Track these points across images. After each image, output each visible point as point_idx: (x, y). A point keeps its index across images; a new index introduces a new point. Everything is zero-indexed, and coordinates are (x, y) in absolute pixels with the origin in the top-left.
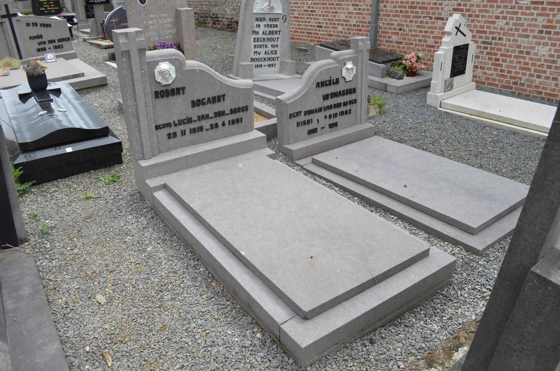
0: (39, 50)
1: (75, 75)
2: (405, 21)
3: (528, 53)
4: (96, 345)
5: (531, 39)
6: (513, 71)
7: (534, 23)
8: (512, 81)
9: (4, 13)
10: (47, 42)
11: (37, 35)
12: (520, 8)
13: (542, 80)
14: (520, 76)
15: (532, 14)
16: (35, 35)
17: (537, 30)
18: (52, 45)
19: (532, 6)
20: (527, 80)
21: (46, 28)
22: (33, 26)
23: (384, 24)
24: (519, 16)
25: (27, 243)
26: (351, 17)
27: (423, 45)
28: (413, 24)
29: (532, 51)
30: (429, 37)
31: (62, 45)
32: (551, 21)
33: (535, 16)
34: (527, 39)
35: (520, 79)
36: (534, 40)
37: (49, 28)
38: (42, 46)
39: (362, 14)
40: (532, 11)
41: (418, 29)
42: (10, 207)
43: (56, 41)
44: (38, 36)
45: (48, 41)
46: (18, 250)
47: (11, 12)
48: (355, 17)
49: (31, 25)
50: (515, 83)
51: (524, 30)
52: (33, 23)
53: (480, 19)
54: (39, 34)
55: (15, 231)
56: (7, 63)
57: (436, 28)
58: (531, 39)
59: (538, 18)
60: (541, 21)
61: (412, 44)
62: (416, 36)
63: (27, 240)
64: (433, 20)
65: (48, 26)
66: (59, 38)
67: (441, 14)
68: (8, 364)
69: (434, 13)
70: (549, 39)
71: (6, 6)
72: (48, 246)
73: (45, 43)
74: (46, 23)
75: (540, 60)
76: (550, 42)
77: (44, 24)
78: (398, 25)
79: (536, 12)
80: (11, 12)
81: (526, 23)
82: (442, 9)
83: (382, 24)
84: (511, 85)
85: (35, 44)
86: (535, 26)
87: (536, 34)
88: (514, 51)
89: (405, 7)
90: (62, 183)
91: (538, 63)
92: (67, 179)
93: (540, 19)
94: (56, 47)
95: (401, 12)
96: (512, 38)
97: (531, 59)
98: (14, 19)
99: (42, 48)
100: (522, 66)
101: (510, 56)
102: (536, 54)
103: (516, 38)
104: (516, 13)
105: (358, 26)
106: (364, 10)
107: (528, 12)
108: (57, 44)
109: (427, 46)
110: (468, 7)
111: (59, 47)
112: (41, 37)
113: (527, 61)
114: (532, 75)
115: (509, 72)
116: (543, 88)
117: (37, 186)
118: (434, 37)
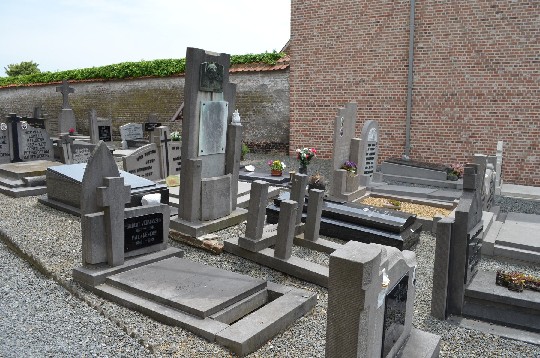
2: (432, 144)
3: (523, 160)
5: (524, 152)
6: (515, 171)
7: (525, 143)
8: (514, 177)
12: (515, 135)
13: (534, 175)
14: (519, 174)
15: (523, 139)
17: (527, 147)
19: (523, 134)
20: (524, 176)
23: (414, 146)
24: (515, 140)
26: (385, 142)
27: (447, 159)
28: (439, 146)
29: (526, 159)
30: (452, 154)
32: (535, 142)
33: (525, 140)
34: (521, 153)
35: (520, 175)
36: (526, 153)
39: (395, 139)
40: (523, 137)
41: (443, 149)
47: (168, 138)
48: (388, 142)
49: (175, 148)
50: (517, 178)
51: (519, 148)
52: (177, 147)
53: (488, 142)
56: (172, 180)
57: (457, 148)
58: (524, 152)
59: (527, 141)
60: (529, 142)
61: (439, 158)
62: (442, 153)
64: (454, 143)
67: (460, 139)
69: (455, 139)
70: (535, 152)
71: (165, 133)
75: (531, 164)
76: (536, 154)
78: (427, 146)
79: (525, 137)
80: (168, 138)
81: (520, 144)
82: (461, 136)
83: (413, 146)
84: (514, 180)
86: (526, 145)
87: (527, 149)
88: (514, 160)
89: (432, 135)
91: (530, 166)
93: (528, 141)
95: (429, 138)
96: (511, 153)
97: (525, 164)
98: (168, 143)
100: (520, 168)
101: (511, 163)
102: (528, 161)
103: (514, 152)
104: (513, 138)
105: (391, 147)
106: (396, 137)
107: (520, 137)
109: (451, 159)
110: (480, 135)
113: (523, 165)
114: (527, 173)
115: (512, 172)
116: (535, 180)
118: (455, 154)
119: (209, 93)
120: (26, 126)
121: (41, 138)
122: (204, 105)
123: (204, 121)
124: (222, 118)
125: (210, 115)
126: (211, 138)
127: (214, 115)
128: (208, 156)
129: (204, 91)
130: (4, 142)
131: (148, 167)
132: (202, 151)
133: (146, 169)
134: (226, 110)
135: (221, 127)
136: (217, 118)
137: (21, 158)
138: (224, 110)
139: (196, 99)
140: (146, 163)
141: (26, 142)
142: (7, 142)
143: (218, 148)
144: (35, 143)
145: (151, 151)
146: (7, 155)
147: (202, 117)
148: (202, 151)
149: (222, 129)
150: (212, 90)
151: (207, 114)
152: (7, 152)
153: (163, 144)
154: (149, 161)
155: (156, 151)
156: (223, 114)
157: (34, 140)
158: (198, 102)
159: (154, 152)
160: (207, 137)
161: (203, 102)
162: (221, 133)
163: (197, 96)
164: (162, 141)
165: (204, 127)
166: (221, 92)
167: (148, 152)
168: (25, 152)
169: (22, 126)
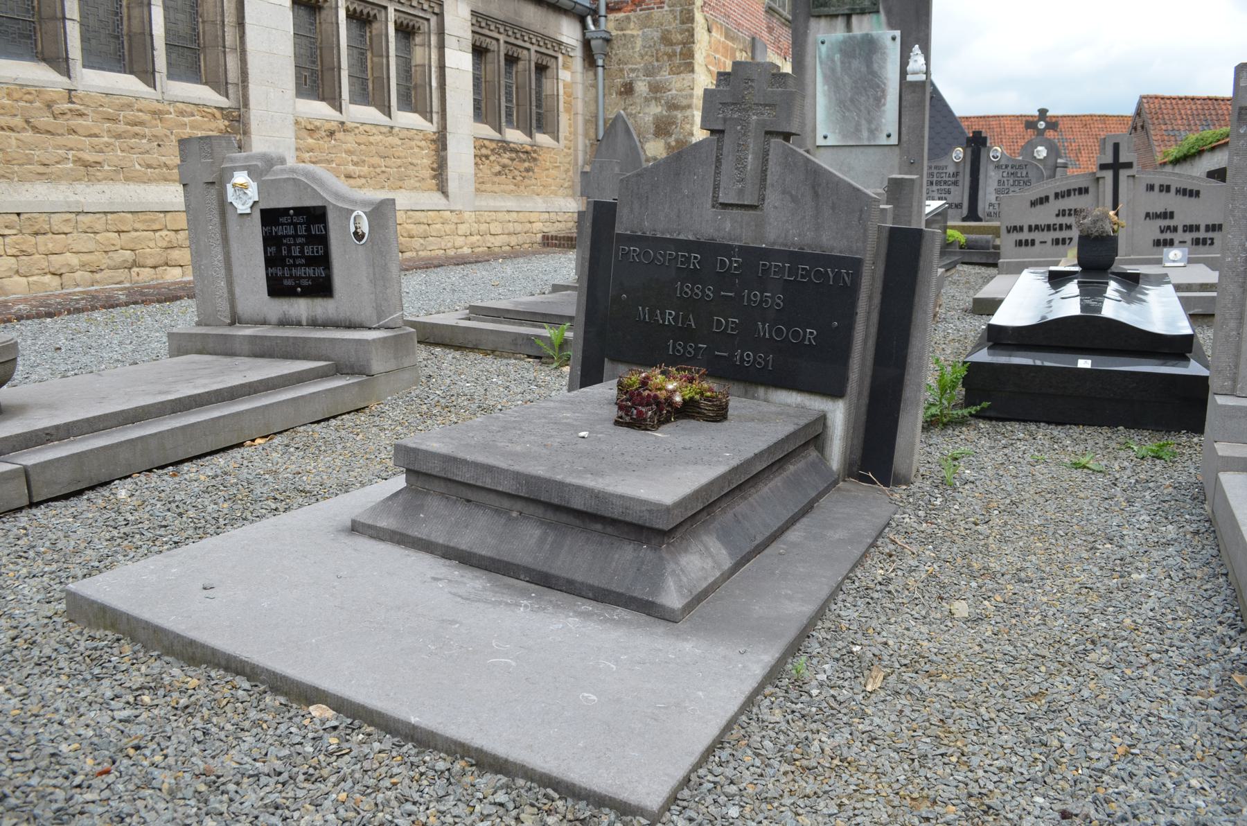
0: (1157, 243)
1: (1207, 284)
4: (877, 653)
9: (1109, 159)
10: (1180, 229)
11: (1163, 210)
16: (1160, 210)
18: (1188, 237)
21: (1186, 198)
22: (1161, 191)
25: (904, 487)
31: (1212, 239)
37: (1193, 199)
38: (1168, 236)
42: (900, 401)
43: (1202, 228)
44: (1165, 213)
45: (1184, 226)
46: (883, 491)
47: (1122, 159)
49: (1157, 188)
52: (1161, 186)
54: (1168, 210)
55: (893, 452)
63: (908, 482)
65: (1194, 194)
66: (1210, 223)
68: (706, 579)
71: (1116, 147)
72: (938, 503)
73: (1175, 229)
74: (1189, 188)
77: (1185, 190)
80: (1122, 159)
85: (1153, 230)
90: (1043, 433)
92: (1060, 428)
94: (1197, 242)
99: (1165, 240)
108: (1202, 234)
111: (1204, 242)
112: (1171, 215)
117: (994, 423)
119: (840, 19)
120: (999, 155)
121: (1026, 179)
122: (823, 43)
123: (825, 76)
124: (882, 67)
125: (842, 63)
126: (849, 110)
127: (856, 64)
128: (847, 149)
129: (826, 16)
130: (955, 183)
131: (1061, 226)
132: (825, 137)
133: (1055, 230)
134: (893, 52)
135: (879, 86)
136: (864, 69)
137: (980, 214)
138: (887, 51)
139: (805, 34)
140: (1058, 215)
141: (995, 185)
142: (960, 183)
143: (872, 132)
144: (1012, 189)
145: (1075, 190)
146: (956, 206)
147: (821, 68)
148: (825, 137)
149: (883, 91)
150: (847, 12)
151: (833, 61)
152: (957, 201)
153: (1109, 175)
154: (1064, 210)
155: (1090, 190)
156: (884, 60)
157: (1011, 182)
158: (810, 39)
159: (1083, 191)
160: (837, 108)
161: (821, 37)
162: (879, 100)
163: (807, 27)
164: (1103, 167)
165: (826, 87)
166: (878, 12)
167: (1065, 189)
168: (991, 205)
169: (991, 155)
